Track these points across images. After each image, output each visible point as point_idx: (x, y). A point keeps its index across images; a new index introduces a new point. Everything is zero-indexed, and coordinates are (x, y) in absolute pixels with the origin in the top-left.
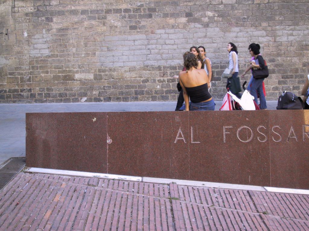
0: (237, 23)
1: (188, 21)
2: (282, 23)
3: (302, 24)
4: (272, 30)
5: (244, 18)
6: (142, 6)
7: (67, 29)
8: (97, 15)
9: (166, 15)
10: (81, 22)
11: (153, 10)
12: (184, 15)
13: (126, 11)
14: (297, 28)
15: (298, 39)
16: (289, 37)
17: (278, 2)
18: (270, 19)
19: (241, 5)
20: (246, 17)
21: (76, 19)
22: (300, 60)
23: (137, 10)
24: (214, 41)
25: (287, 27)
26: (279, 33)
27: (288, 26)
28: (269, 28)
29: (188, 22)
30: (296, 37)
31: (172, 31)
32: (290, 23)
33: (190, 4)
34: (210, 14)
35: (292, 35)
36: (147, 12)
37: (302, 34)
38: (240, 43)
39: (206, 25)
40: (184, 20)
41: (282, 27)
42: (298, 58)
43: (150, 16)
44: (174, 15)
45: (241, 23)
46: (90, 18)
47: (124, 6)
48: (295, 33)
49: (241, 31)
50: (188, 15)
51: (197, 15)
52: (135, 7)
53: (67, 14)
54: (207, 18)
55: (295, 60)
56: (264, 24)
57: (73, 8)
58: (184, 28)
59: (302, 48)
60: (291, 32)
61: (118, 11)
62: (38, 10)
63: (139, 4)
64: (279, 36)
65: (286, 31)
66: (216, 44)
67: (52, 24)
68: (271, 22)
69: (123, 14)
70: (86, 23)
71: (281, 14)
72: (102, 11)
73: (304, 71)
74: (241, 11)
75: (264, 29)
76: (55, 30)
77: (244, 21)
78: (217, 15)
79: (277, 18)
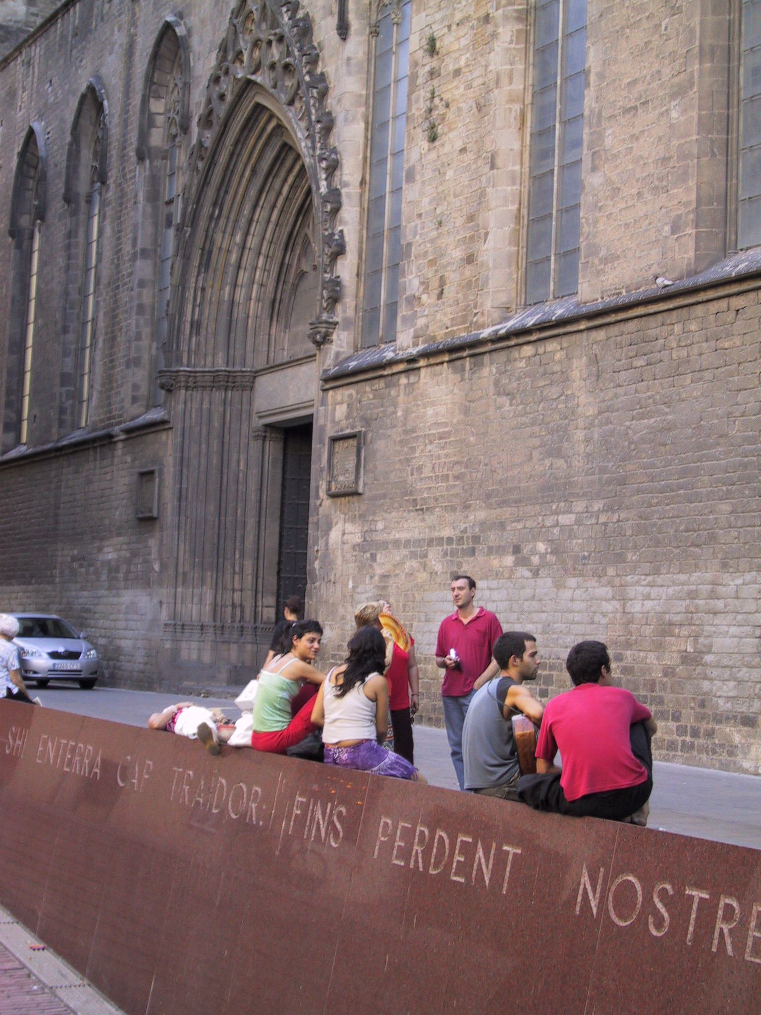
0: (575, 569)
1: (517, 563)
2: (635, 568)
3: (665, 571)
4: (621, 585)
5: (584, 558)
6: (465, 531)
7: (388, 576)
8: (419, 549)
9: (490, 551)
10: (401, 563)
11: (476, 539)
12: (511, 550)
13: (450, 540)
14: (659, 580)
15: (658, 609)
16: (645, 602)
17: (633, 520)
18: (620, 558)
19: (581, 528)
20: (586, 554)
21: (397, 555)
22: (658, 659)
23: (460, 540)
24: (544, 609)
25: (643, 577)
26: (631, 592)
27: (645, 575)
28: (617, 581)
29: (515, 565)
30: (655, 602)
31: (494, 584)
32: (647, 567)
33: (520, 526)
34: (541, 547)
35: (647, 597)
36: (471, 545)
37: (664, 597)
38: (576, 614)
39: (536, 574)
40: (509, 560)
41: (636, 578)
42: (656, 653)
43: (473, 552)
44: (499, 551)
45: (580, 567)
46: (414, 555)
47: (447, 533)
48: (654, 592)
49: (578, 587)
50: (517, 550)
51: (526, 551)
52: (458, 532)
53: (390, 546)
54: (537, 557)
55: (651, 657)
56: (611, 571)
57: (397, 536)
58: (509, 578)
59: (664, 631)
60: (648, 589)
61: (440, 541)
62: (365, 540)
63: (463, 526)
64: (631, 600)
65: (640, 589)
66: (545, 614)
67: (374, 564)
68: (620, 566)
69: (445, 547)
70: (407, 565)
71: (635, 547)
72: (424, 540)
73: (664, 687)
74: (580, 541)
75: (610, 583)
76: (377, 578)
77: (584, 564)
78: (549, 550)
79: (630, 556)
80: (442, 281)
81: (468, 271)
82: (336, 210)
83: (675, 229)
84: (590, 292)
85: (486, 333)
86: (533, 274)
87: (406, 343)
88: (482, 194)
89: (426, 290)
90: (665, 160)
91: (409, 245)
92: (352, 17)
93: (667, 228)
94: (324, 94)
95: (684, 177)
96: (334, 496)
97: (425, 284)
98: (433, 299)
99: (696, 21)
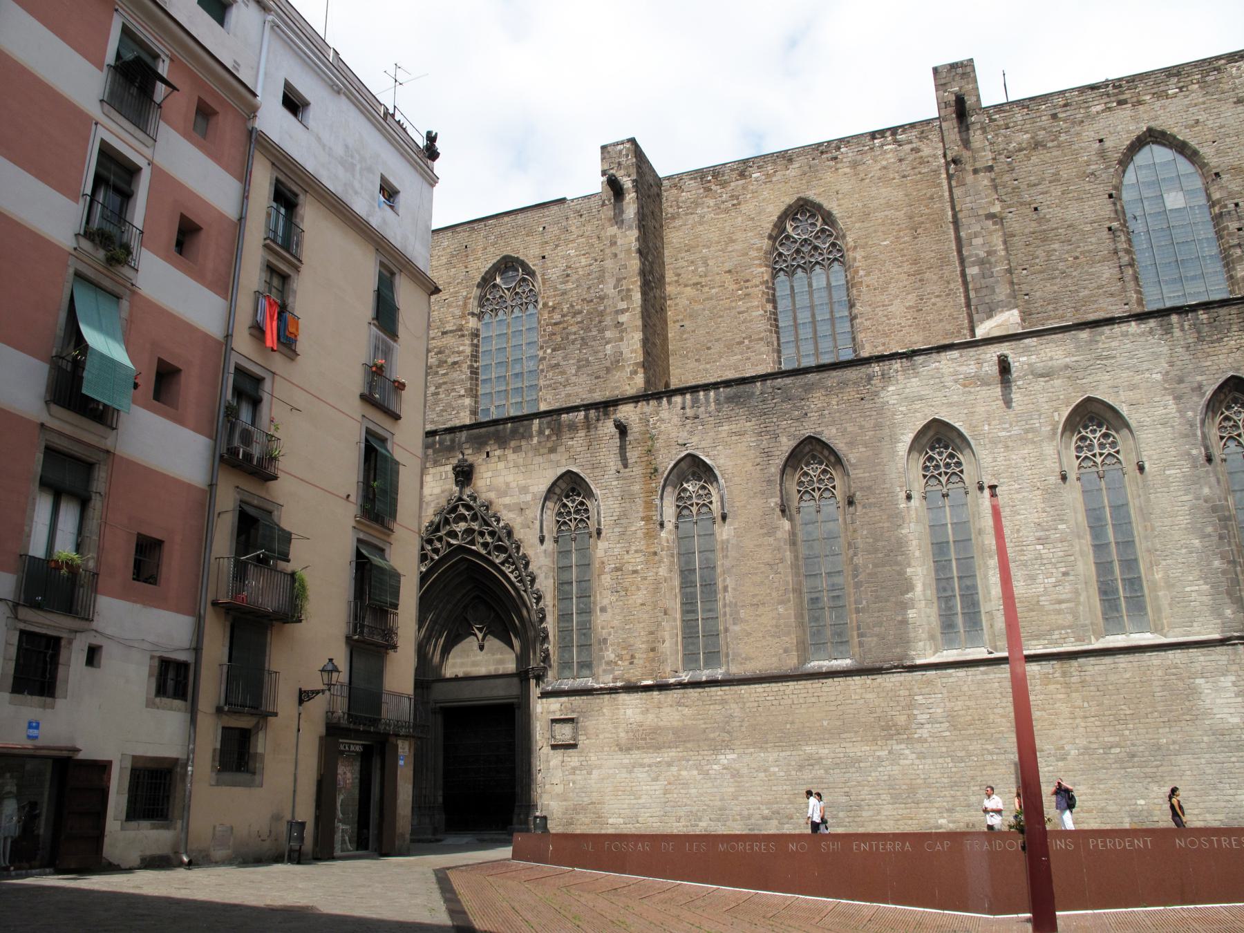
80: (633, 657)
81: (651, 654)
82: (544, 617)
83: (786, 651)
84: (736, 670)
85: (672, 681)
86: (690, 659)
87: (606, 681)
88: (659, 624)
89: (621, 659)
90: (777, 626)
91: (605, 640)
92: (545, 533)
93: (781, 651)
94: (527, 565)
95: (789, 633)
96: (554, 747)
97: (620, 657)
98: (627, 663)
99: (790, 579)
